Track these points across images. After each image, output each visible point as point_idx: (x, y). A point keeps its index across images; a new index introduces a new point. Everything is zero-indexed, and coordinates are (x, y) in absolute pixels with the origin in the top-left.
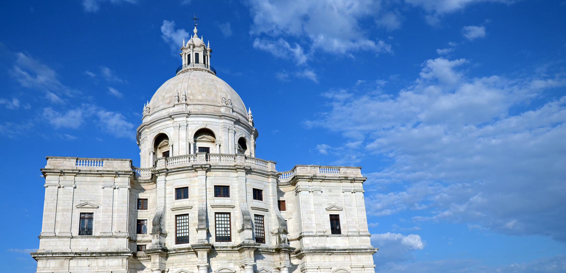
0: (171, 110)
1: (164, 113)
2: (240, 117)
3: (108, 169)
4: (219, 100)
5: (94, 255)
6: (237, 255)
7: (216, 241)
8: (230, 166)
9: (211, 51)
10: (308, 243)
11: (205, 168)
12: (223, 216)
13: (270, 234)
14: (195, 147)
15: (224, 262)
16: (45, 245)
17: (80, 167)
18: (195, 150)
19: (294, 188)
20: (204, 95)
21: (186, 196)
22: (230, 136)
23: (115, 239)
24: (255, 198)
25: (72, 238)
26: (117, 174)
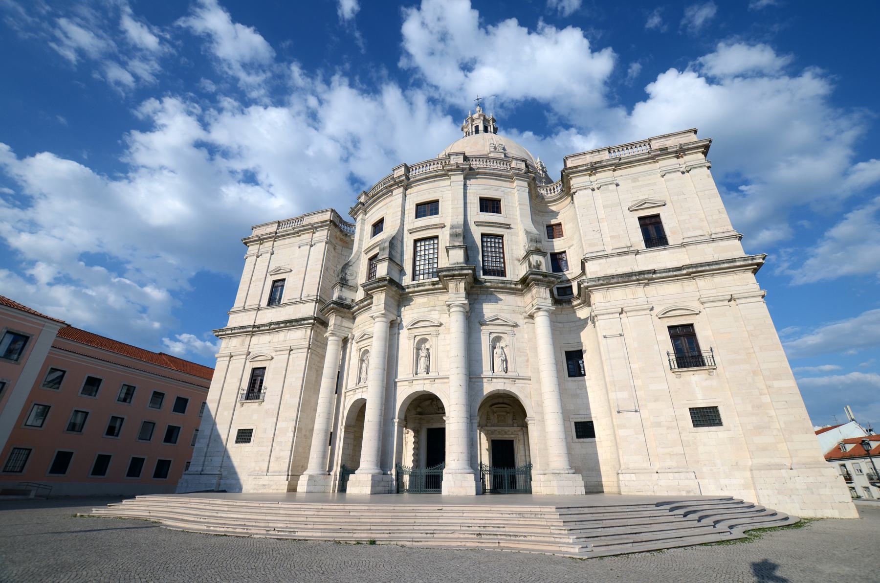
13: (516, 262)
15: (423, 310)
23: (301, 305)
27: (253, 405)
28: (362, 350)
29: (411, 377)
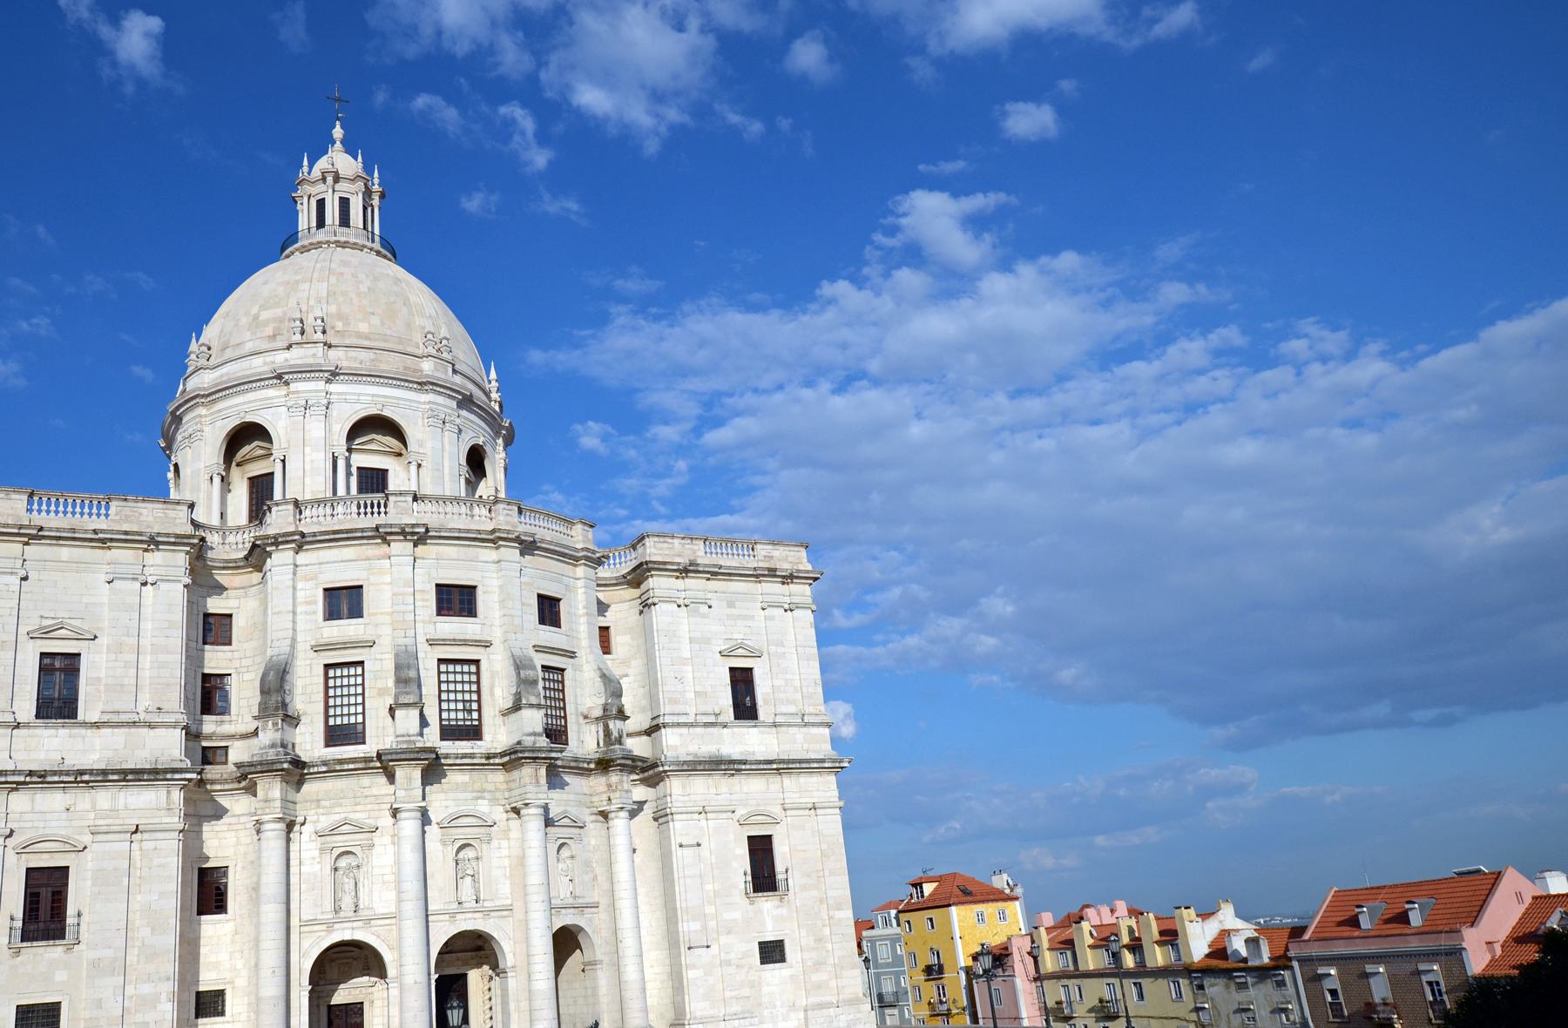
0: (281, 359)
1: (259, 365)
3: (126, 527)
4: (418, 338)
5: (86, 778)
6: (499, 777)
7: (442, 739)
8: (479, 532)
9: (382, 196)
10: (675, 744)
11: (413, 534)
12: (458, 668)
14: (348, 466)
17: (39, 519)
18: (349, 474)
19: (636, 592)
20: (375, 321)
21: (356, 612)
22: (446, 440)
23: (145, 730)
24: (542, 621)
25: (18, 726)
26: (153, 542)
27: (47, 953)
28: (337, 852)
29: (455, 905)
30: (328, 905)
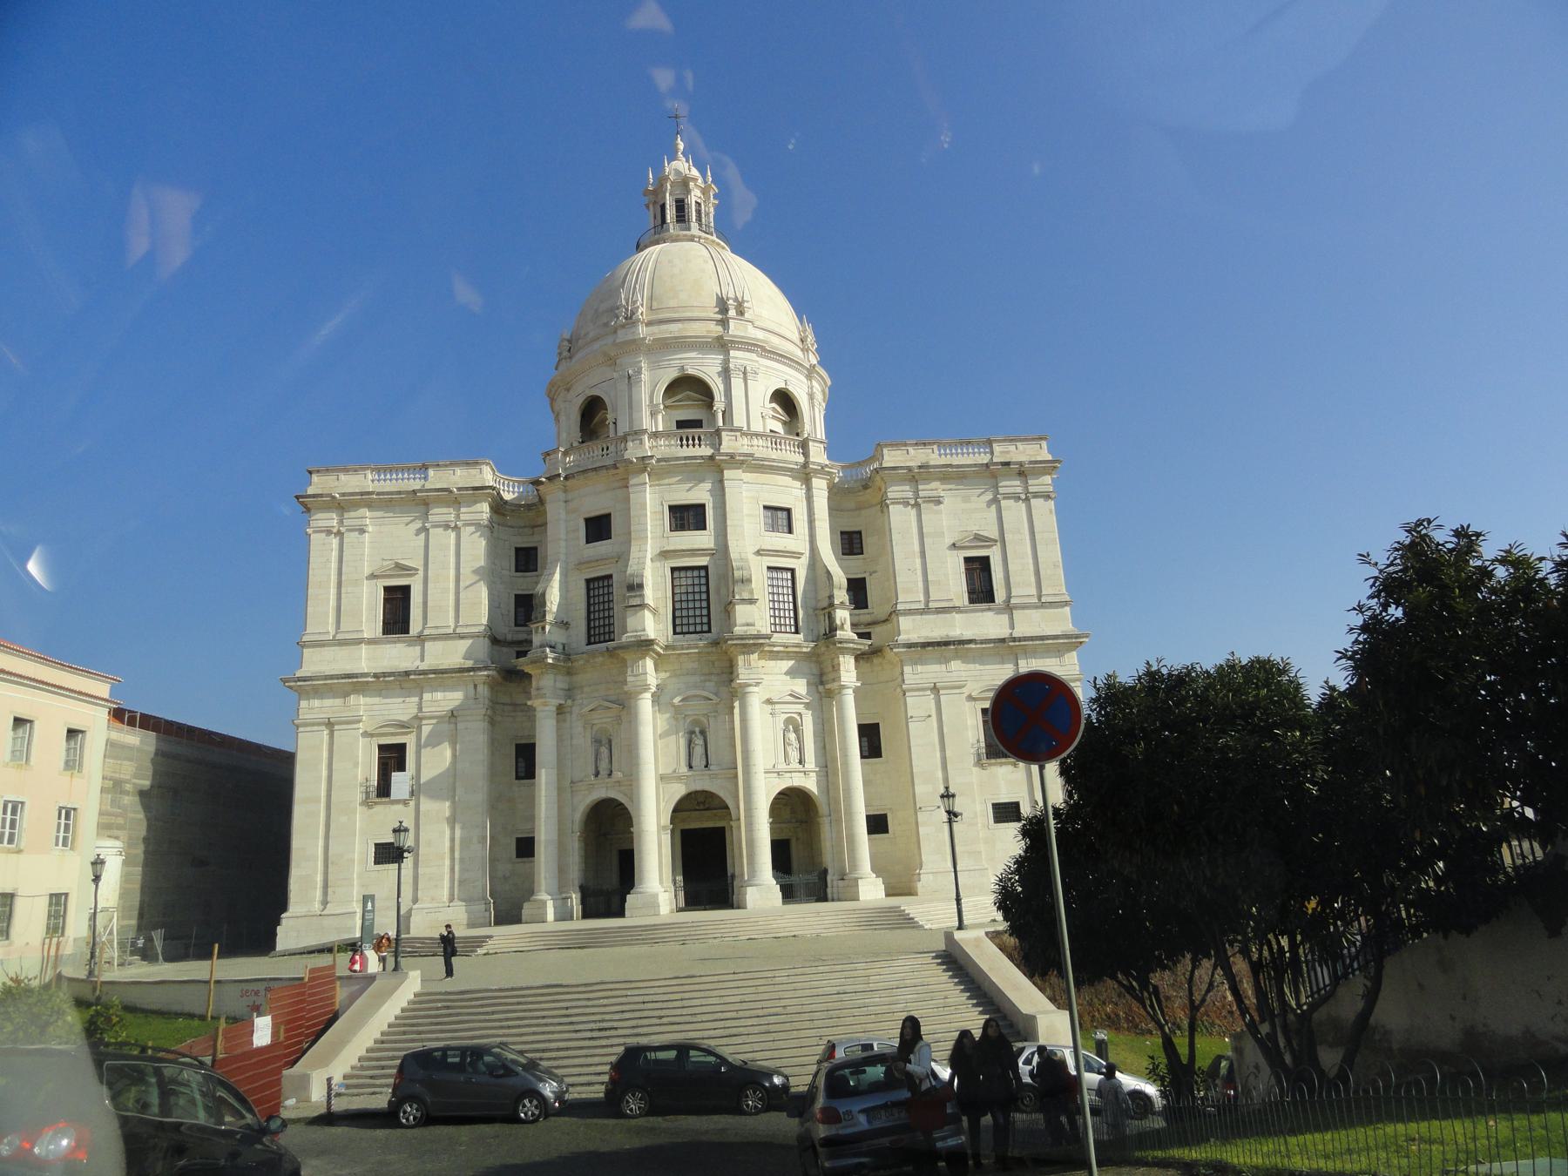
2: (775, 341)
12: (689, 574)
16: (316, 663)
30: (591, 769)
